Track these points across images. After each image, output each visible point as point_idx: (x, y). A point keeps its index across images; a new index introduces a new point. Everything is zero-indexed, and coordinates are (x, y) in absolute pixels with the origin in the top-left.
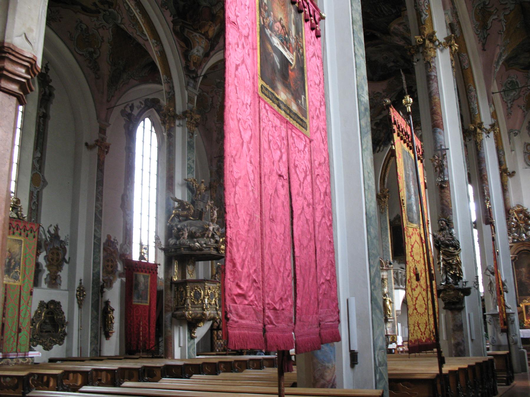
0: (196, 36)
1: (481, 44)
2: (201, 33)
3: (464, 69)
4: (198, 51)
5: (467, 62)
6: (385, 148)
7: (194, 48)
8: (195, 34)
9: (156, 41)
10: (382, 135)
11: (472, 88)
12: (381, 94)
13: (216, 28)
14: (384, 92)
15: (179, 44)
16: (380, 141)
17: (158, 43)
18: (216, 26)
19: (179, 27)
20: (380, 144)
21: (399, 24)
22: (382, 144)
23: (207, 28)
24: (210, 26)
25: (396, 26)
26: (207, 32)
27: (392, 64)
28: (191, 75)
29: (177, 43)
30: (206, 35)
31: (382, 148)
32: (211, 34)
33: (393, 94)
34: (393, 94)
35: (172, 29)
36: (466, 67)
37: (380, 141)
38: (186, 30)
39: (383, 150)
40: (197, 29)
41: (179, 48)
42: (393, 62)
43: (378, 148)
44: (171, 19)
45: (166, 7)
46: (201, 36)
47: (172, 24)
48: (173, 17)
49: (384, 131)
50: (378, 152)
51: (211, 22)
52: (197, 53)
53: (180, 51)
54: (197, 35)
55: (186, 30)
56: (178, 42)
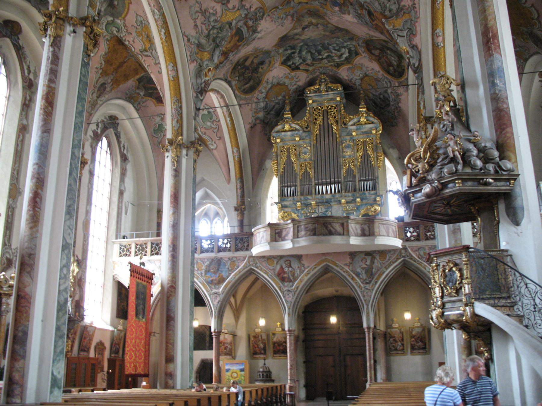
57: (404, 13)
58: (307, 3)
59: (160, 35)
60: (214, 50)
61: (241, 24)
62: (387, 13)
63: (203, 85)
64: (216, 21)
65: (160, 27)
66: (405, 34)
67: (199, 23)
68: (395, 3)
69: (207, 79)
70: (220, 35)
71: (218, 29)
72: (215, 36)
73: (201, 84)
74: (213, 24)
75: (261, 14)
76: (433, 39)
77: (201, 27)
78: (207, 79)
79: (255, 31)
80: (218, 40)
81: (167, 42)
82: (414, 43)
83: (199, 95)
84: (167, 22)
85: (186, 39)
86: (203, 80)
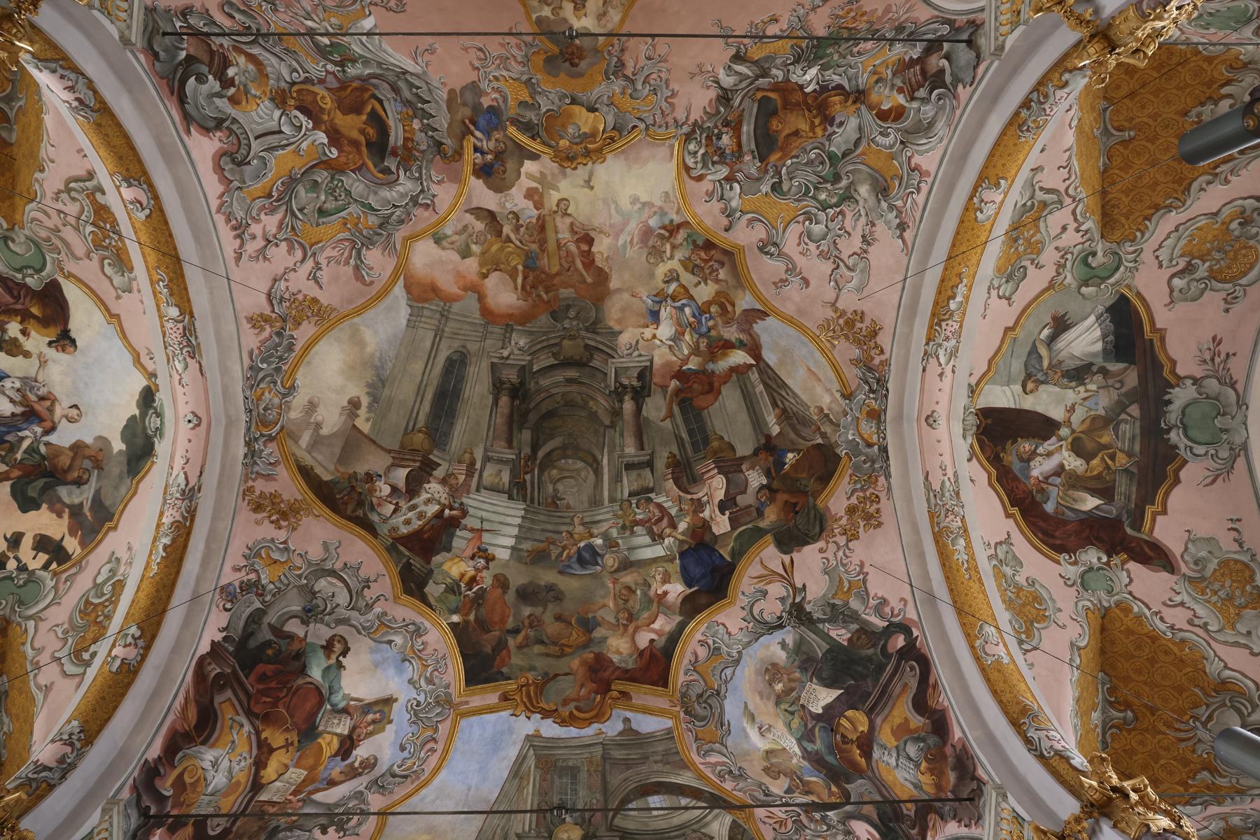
0: (242, 726)
2: (258, 733)
4: (215, 764)
7: (212, 747)
8: (244, 721)
9: (138, 634)
17: (141, 643)
24: (287, 745)
26: (272, 750)
28: (146, 801)
29: (182, 691)
38: (229, 693)
40: (257, 716)
44: (219, 637)
45: (228, 606)
47: (208, 649)
48: (225, 638)
52: (207, 765)
53: (171, 717)
54: (247, 727)
56: (187, 692)
57: (270, 196)
58: (574, 101)
59: (967, 298)
60: (845, 155)
61: (751, 165)
62: (322, 176)
63: (922, 93)
64: (809, 217)
65: (956, 318)
66: (254, 144)
67: (857, 243)
68: (301, 210)
69: (901, 99)
70: (814, 179)
71: (814, 198)
72: (828, 186)
73: (925, 101)
74: (822, 216)
75: (692, 147)
76: (151, 188)
77: (854, 228)
78: (901, 99)
79: (725, 97)
80: (826, 170)
81: (959, 275)
82: (218, 134)
83: (948, 79)
84: (933, 315)
85: (908, 235)
86: (915, 105)
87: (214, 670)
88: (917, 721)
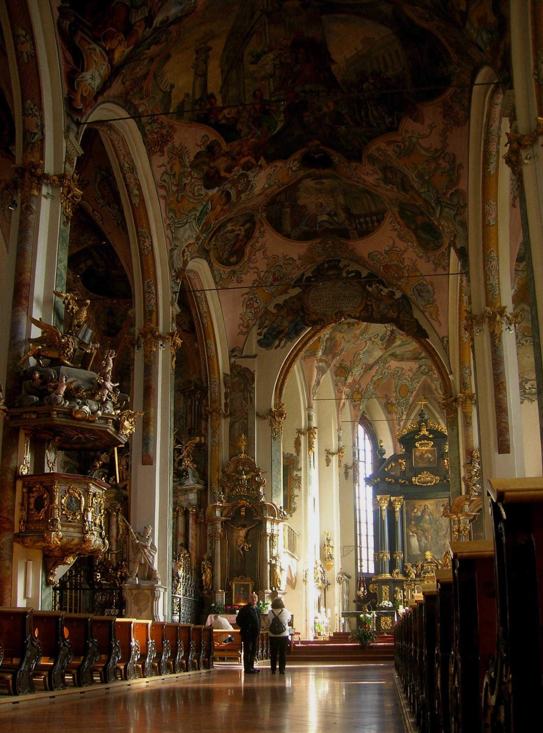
1: (512, 197)
3: (488, 225)
5: (494, 215)
6: (288, 343)
10: (286, 324)
11: (494, 254)
12: (295, 260)
13: (127, 51)
14: (299, 259)
15: (63, 53)
16: (281, 332)
17: (28, 37)
18: (128, 47)
19: (69, 22)
20: (280, 336)
21: (388, 144)
22: (284, 337)
23: (115, 43)
25: (383, 145)
27: (325, 217)
30: (110, 53)
31: (283, 343)
32: (117, 56)
33: (310, 266)
34: (310, 266)
35: (56, 22)
36: (492, 223)
37: (281, 332)
38: (80, 34)
39: (284, 346)
41: (62, 59)
42: (329, 214)
43: (277, 342)
46: (103, 53)
49: (289, 318)
50: (276, 348)
51: (122, 36)
55: (80, 34)
87: (66, 24)
88: (492, 19)
